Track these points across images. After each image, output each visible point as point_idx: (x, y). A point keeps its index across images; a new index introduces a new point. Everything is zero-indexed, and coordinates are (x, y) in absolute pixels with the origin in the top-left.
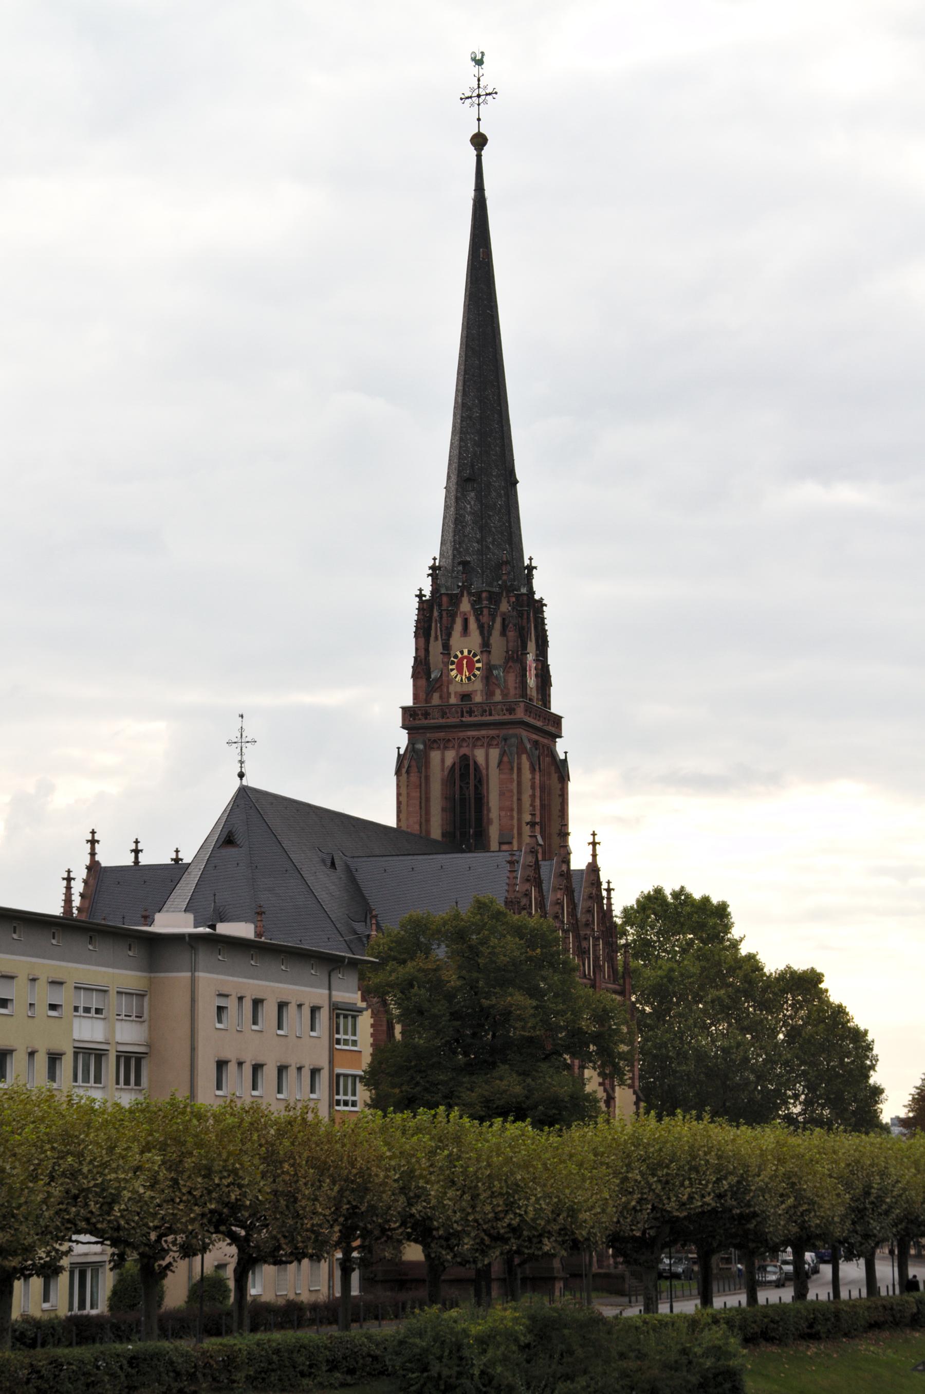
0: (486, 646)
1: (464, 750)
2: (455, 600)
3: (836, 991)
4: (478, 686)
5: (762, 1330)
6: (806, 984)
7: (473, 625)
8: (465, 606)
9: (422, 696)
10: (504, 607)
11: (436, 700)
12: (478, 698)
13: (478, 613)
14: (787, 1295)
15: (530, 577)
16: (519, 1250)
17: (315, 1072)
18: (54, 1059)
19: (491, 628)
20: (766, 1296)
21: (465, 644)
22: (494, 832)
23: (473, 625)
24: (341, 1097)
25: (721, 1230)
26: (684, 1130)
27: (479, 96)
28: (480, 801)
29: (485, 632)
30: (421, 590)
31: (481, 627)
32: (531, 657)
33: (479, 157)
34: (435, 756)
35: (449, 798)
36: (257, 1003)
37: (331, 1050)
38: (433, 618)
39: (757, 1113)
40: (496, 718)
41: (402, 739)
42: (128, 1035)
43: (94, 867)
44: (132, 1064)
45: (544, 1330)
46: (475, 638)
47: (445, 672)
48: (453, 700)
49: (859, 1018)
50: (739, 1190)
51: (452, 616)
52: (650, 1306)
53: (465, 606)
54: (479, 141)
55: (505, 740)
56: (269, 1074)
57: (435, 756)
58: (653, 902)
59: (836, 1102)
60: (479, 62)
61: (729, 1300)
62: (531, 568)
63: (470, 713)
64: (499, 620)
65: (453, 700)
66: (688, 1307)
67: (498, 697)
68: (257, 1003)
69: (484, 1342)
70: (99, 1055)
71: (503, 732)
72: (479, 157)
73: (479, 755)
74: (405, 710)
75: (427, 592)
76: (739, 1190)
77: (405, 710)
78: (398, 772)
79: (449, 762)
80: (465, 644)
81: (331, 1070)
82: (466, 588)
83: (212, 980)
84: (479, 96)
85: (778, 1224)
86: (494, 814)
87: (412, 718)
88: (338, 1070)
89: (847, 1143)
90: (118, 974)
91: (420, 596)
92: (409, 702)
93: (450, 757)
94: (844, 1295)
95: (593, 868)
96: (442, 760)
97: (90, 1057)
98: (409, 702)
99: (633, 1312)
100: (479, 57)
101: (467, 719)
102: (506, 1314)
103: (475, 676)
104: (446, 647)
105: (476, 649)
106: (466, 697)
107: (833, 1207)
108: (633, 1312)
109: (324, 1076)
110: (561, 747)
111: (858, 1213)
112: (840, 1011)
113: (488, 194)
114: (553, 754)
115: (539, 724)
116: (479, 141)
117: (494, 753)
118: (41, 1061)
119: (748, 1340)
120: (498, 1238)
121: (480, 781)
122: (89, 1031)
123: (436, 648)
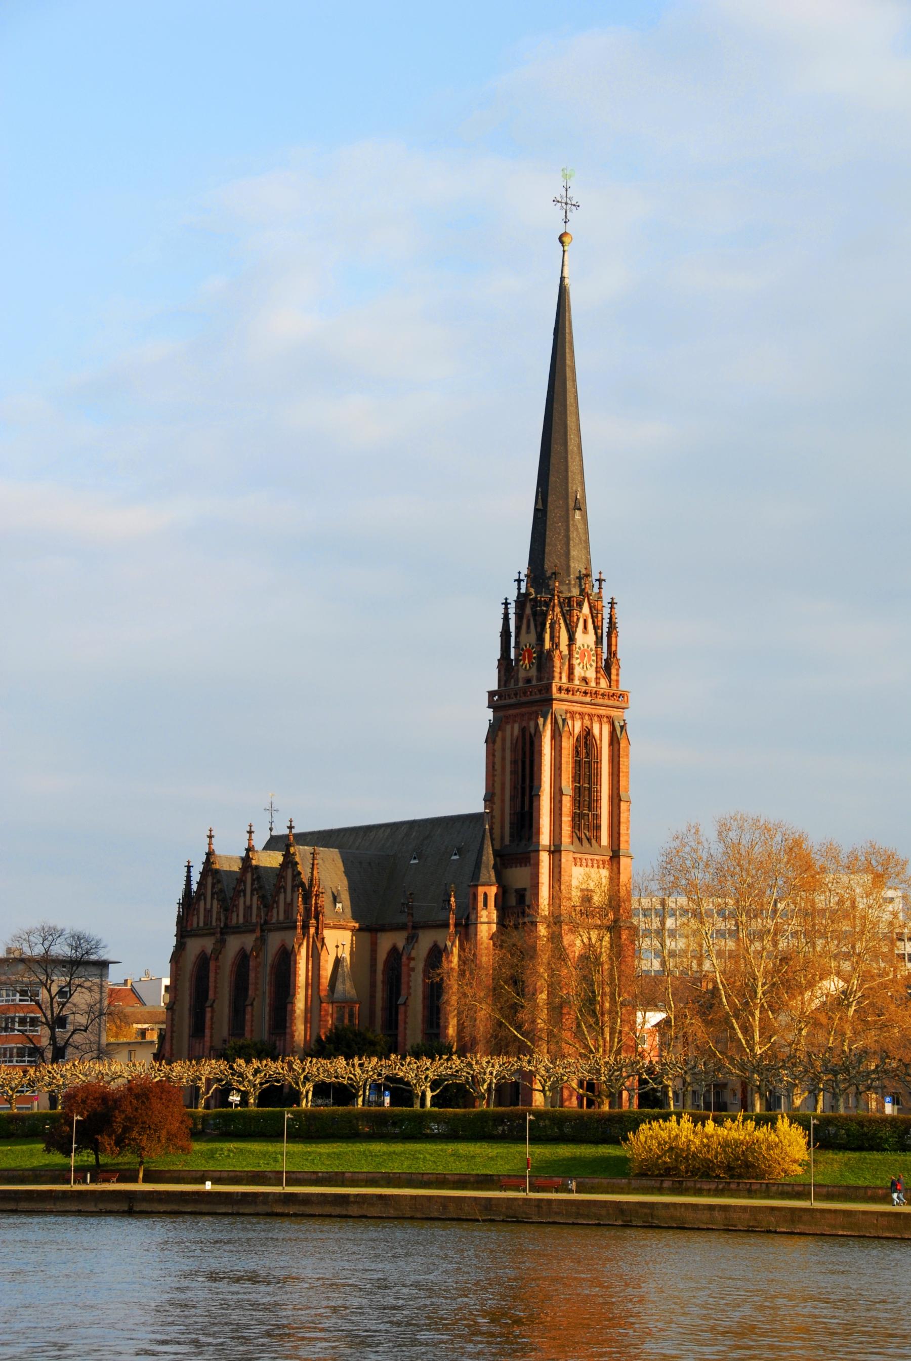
1: (524, 724)
4: (533, 672)
9: (503, 683)
12: (534, 682)
27: (567, 204)
30: (506, 599)
33: (564, 251)
41: (489, 714)
57: (508, 727)
65: (521, 684)
74: (491, 694)
77: (491, 694)
78: (486, 742)
87: (497, 701)
91: (506, 604)
92: (495, 687)
98: (495, 687)
103: (533, 663)
106: (528, 681)
113: (567, 281)
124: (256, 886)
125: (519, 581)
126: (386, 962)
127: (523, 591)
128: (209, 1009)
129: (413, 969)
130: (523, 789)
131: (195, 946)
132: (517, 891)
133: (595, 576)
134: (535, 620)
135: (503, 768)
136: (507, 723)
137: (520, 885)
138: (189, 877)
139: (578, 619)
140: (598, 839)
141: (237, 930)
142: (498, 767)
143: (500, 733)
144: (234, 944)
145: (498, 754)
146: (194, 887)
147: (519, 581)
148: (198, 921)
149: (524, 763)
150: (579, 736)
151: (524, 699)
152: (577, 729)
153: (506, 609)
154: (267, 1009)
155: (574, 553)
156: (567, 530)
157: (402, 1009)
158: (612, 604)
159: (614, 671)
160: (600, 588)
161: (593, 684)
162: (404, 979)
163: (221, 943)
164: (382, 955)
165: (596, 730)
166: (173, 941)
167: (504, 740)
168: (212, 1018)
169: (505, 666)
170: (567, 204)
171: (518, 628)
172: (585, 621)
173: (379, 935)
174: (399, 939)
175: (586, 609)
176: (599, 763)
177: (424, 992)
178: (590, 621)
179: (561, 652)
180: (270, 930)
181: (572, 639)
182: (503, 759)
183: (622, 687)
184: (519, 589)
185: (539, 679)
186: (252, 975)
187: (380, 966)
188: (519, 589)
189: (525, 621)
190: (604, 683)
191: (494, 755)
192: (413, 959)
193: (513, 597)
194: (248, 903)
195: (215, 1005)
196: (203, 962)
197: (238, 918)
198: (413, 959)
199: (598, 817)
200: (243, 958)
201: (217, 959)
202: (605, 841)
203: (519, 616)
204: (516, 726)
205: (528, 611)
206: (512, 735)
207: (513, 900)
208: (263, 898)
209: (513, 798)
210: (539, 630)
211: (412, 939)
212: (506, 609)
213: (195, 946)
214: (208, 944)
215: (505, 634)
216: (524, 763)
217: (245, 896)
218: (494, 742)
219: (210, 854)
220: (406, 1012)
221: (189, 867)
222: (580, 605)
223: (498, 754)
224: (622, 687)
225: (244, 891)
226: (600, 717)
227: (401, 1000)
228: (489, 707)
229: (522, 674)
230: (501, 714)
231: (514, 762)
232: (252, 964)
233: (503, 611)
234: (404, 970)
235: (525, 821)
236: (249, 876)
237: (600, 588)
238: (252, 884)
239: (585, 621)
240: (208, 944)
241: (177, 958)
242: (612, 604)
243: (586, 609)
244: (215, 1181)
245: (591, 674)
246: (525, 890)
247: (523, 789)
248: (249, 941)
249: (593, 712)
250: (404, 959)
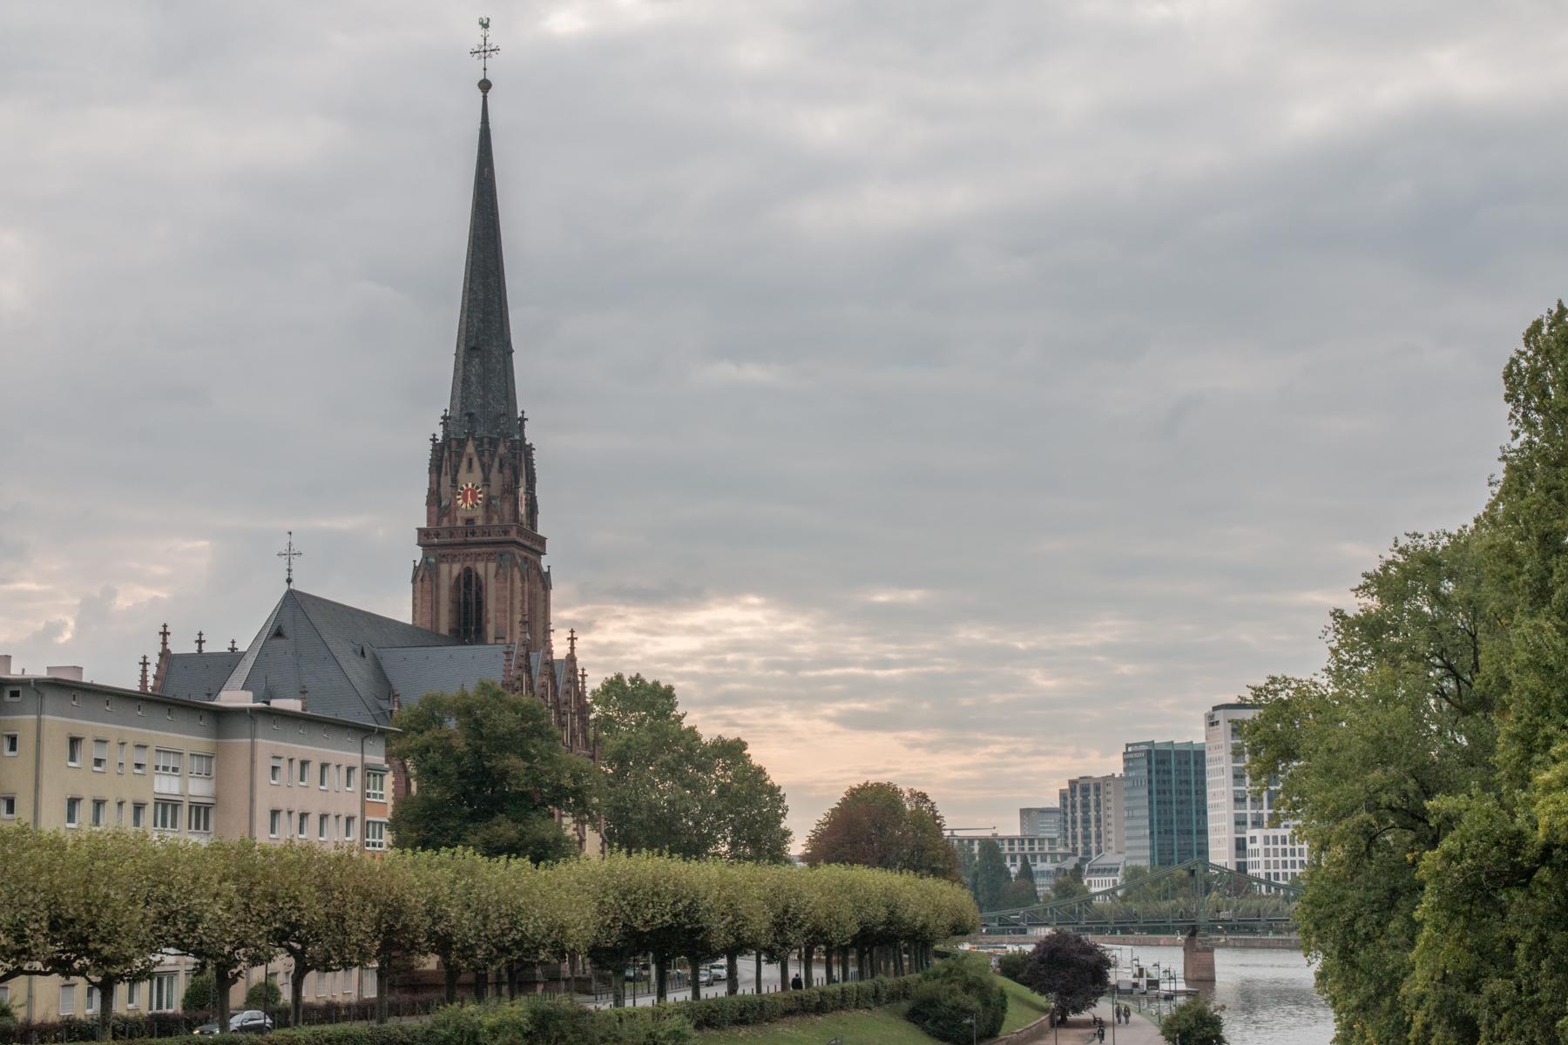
0: (486, 481)
1: (468, 564)
2: (462, 444)
3: (757, 755)
4: (479, 513)
5: (708, 1018)
6: (733, 750)
7: (476, 463)
8: (470, 448)
9: (434, 519)
10: (502, 450)
11: (445, 523)
12: (479, 522)
13: (480, 454)
14: (721, 990)
15: (522, 427)
16: (517, 961)
17: (349, 820)
18: (139, 807)
19: (490, 467)
20: (707, 993)
21: (470, 479)
22: (491, 630)
23: (476, 463)
24: (370, 840)
25: (676, 941)
26: (648, 865)
28: (480, 603)
29: (486, 470)
31: (483, 466)
32: (522, 490)
33: (485, 98)
34: (444, 568)
35: (455, 601)
36: (304, 764)
37: (363, 802)
38: (444, 458)
39: (694, 849)
40: (493, 538)
41: (418, 554)
42: (199, 789)
43: (165, 654)
44: (201, 813)
45: (542, 1021)
46: (478, 473)
47: (453, 501)
48: (459, 523)
49: (775, 777)
50: (690, 911)
51: (460, 456)
52: (619, 1001)
53: (470, 448)
54: (485, 86)
56: (313, 820)
57: (444, 568)
58: (614, 687)
59: (754, 842)
60: (486, 26)
61: (679, 996)
62: (523, 420)
63: (473, 534)
64: (497, 460)
66: (646, 1001)
67: (495, 522)
68: (304, 764)
69: (495, 1031)
70: (176, 805)
71: (499, 549)
72: (485, 98)
73: (480, 568)
75: (440, 437)
76: (690, 911)
78: (414, 580)
79: (456, 572)
80: (470, 479)
81: (363, 818)
82: (471, 434)
83: (269, 745)
84: (485, 51)
85: (719, 938)
86: (491, 615)
87: (425, 537)
88: (368, 818)
89: (769, 874)
90: (190, 739)
91: (434, 440)
93: (457, 569)
94: (764, 990)
95: (571, 658)
96: (450, 571)
97: (167, 806)
98: (424, 525)
99: (605, 1005)
101: (471, 539)
102: (515, 1010)
104: (455, 480)
105: (479, 482)
106: (470, 521)
107: (760, 923)
108: (605, 1005)
109: (357, 823)
110: (544, 562)
111: (779, 927)
112: (761, 771)
114: (539, 568)
115: (528, 543)
116: (485, 86)
117: (492, 566)
118: (128, 809)
119: (698, 1027)
120: (504, 950)
121: (480, 588)
122: (167, 786)
123: (446, 481)
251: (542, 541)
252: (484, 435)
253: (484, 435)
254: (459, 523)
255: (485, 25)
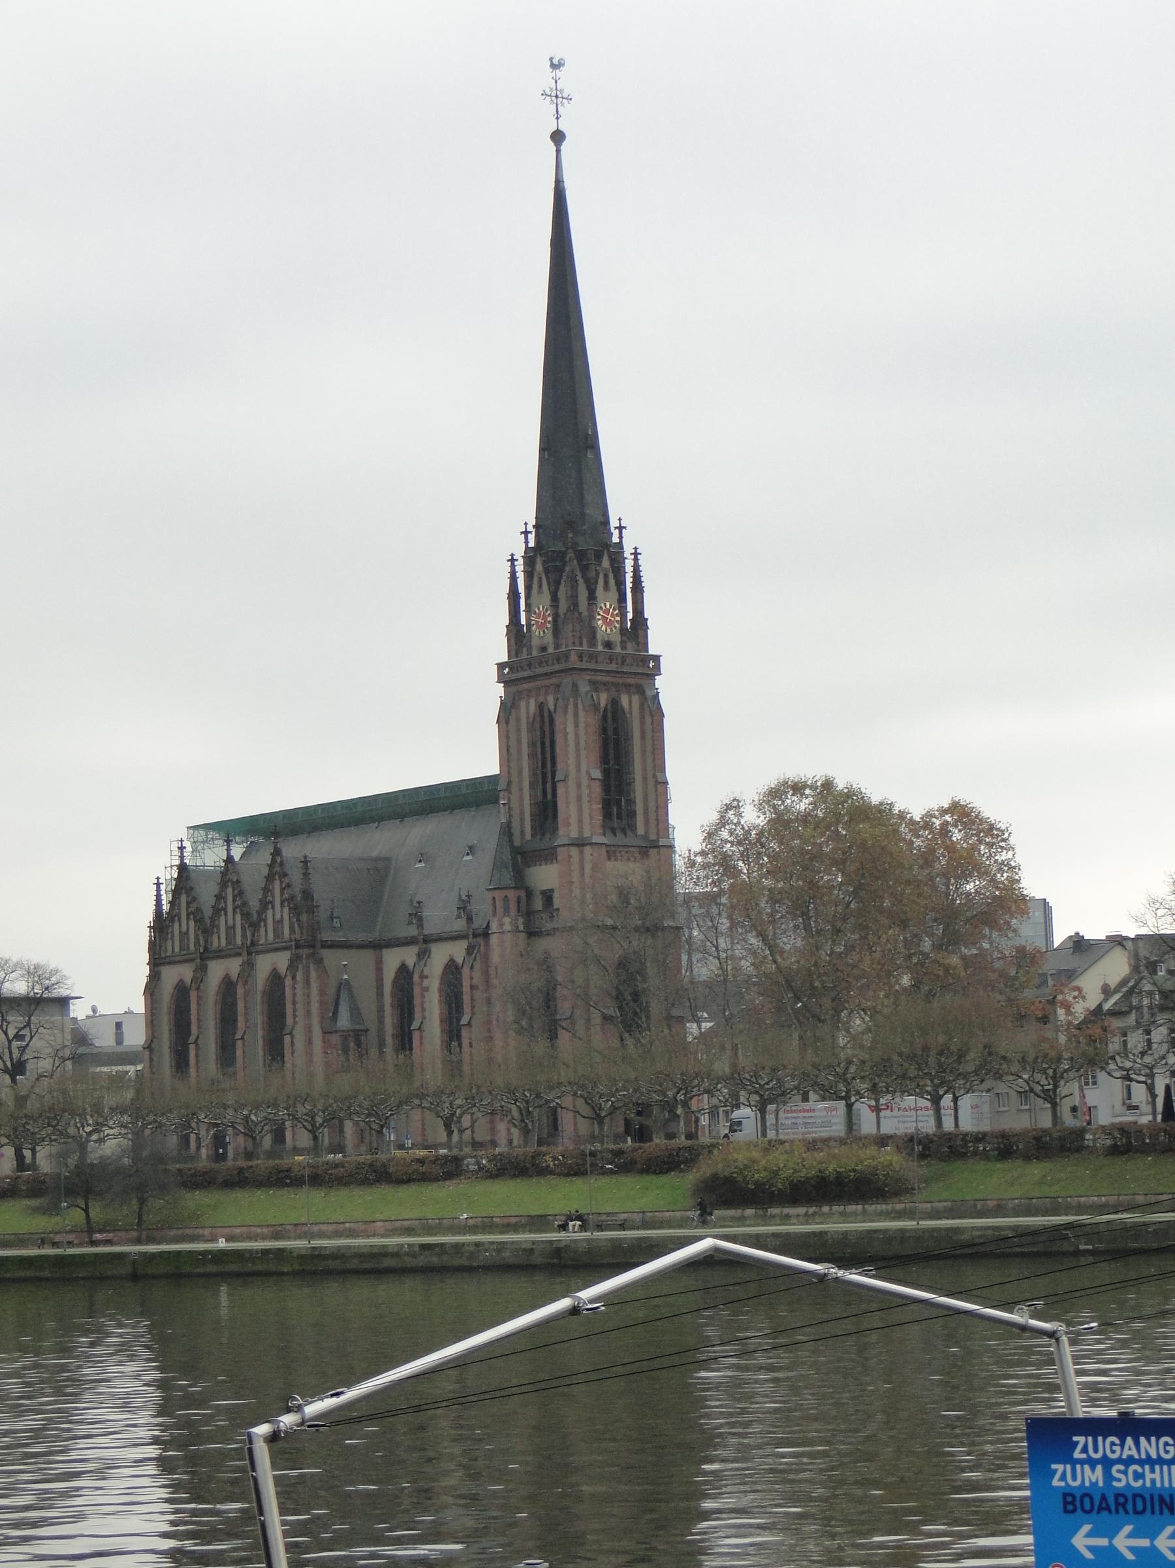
0: (555, 598)
1: (541, 699)
4: (549, 639)
9: (513, 653)
11: (524, 655)
12: (551, 650)
13: (547, 571)
27: (557, 97)
30: (512, 555)
33: (558, 151)
41: (500, 689)
54: (558, 137)
55: (558, 686)
60: (555, 66)
65: (535, 653)
71: (553, 680)
72: (558, 151)
74: (501, 666)
77: (501, 666)
91: (512, 560)
96: (528, 707)
100: (556, 62)
116: (558, 137)
124: (238, 902)
125: (526, 533)
126: (395, 983)
127: (532, 544)
128: (192, 1047)
129: (427, 989)
130: (544, 775)
131: (171, 975)
132: (543, 893)
133: (614, 523)
134: (547, 578)
135: (519, 752)
136: (521, 699)
137: (546, 886)
138: (158, 896)
139: (598, 574)
140: (633, 828)
141: (220, 954)
142: (513, 750)
143: (513, 712)
144: (217, 970)
145: (513, 736)
146: (165, 907)
147: (526, 533)
148: (173, 946)
149: (543, 743)
150: (605, 710)
151: (539, 670)
152: (603, 704)
153: (513, 566)
154: (261, 1042)
155: (588, 498)
156: (579, 471)
157: (416, 1035)
158: (636, 554)
159: (641, 633)
160: (621, 537)
161: (618, 650)
162: (417, 1001)
163: (202, 969)
164: (389, 975)
165: (624, 701)
166: (146, 970)
167: (518, 720)
168: (197, 1056)
169: (516, 634)
170: (557, 97)
171: (528, 588)
172: (606, 576)
173: (385, 952)
174: (409, 956)
175: (606, 563)
176: (629, 738)
177: (441, 1014)
178: (611, 575)
179: (580, 614)
180: (258, 953)
181: (592, 597)
182: (519, 742)
183: (652, 651)
184: (527, 542)
185: (557, 646)
186: (241, 1005)
187: (388, 988)
188: (527, 542)
189: (536, 580)
190: (631, 649)
191: (508, 738)
192: (427, 977)
193: (520, 553)
194: (230, 922)
195: (199, 1042)
196: (182, 992)
197: (219, 940)
198: (427, 977)
199: (631, 802)
200: (228, 986)
201: (198, 989)
202: (641, 830)
203: (529, 575)
204: (532, 702)
205: (539, 567)
206: (528, 713)
207: (538, 904)
208: (246, 915)
209: (532, 786)
210: (553, 588)
211: (423, 955)
212: (513, 566)
213: (171, 975)
214: (186, 972)
215: (513, 595)
216: (543, 743)
217: (226, 914)
218: (507, 722)
219: (182, 867)
220: (421, 1038)
221: (158, 884)
222: (598, 556)
223: (513, 736)
224: (652, 651)
225: (225, 909)
226: (627, 686)
227: (415, 1025)
228: (498, 682)
229: (535, 642)
230: (514, 689)
231: (532, 744)
232: (240, 991)
233: (509, 569)
234: (417, 990)
235: (546, 813)
236: (229, 891)
237: (621, 537)
238: (234, 901)
239: (606, 576)
240: (186, 972)
241: (152, 989)
242: (636, 554)
243: (606, 563)
244: (229, 1239)
245: (616, 638)
246: (552, 890)
247: (544, 775)
248: (233, 966)
249: (621, 681)
250: (416, 977)
251: (656, 658)
252: (574, 547)
253: (574, 547)
254: (535, 653)
255: (555, 66)
